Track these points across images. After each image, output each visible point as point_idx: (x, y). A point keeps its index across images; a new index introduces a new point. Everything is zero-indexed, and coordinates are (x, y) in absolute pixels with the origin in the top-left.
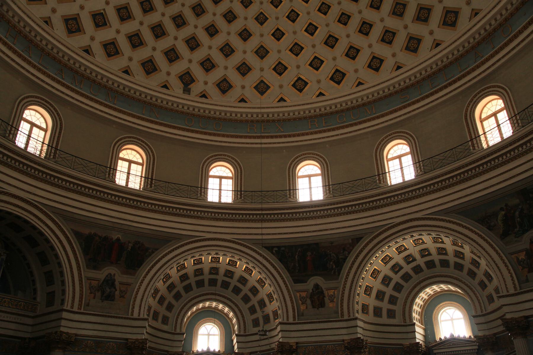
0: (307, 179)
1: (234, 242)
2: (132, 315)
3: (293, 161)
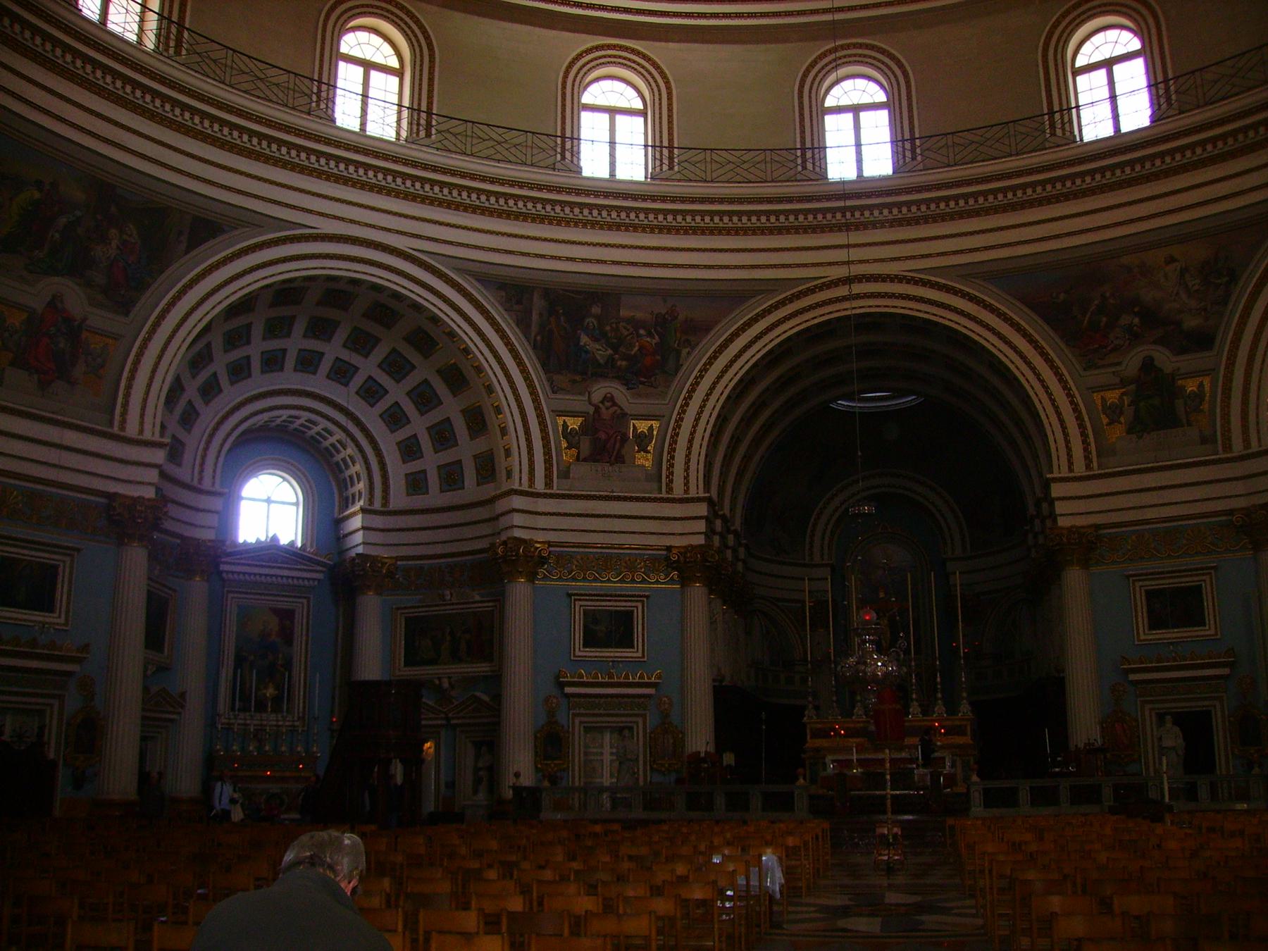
0: (1102, 73)
1: (910, 281)
2: (670, 490)
3: (1055, 26)
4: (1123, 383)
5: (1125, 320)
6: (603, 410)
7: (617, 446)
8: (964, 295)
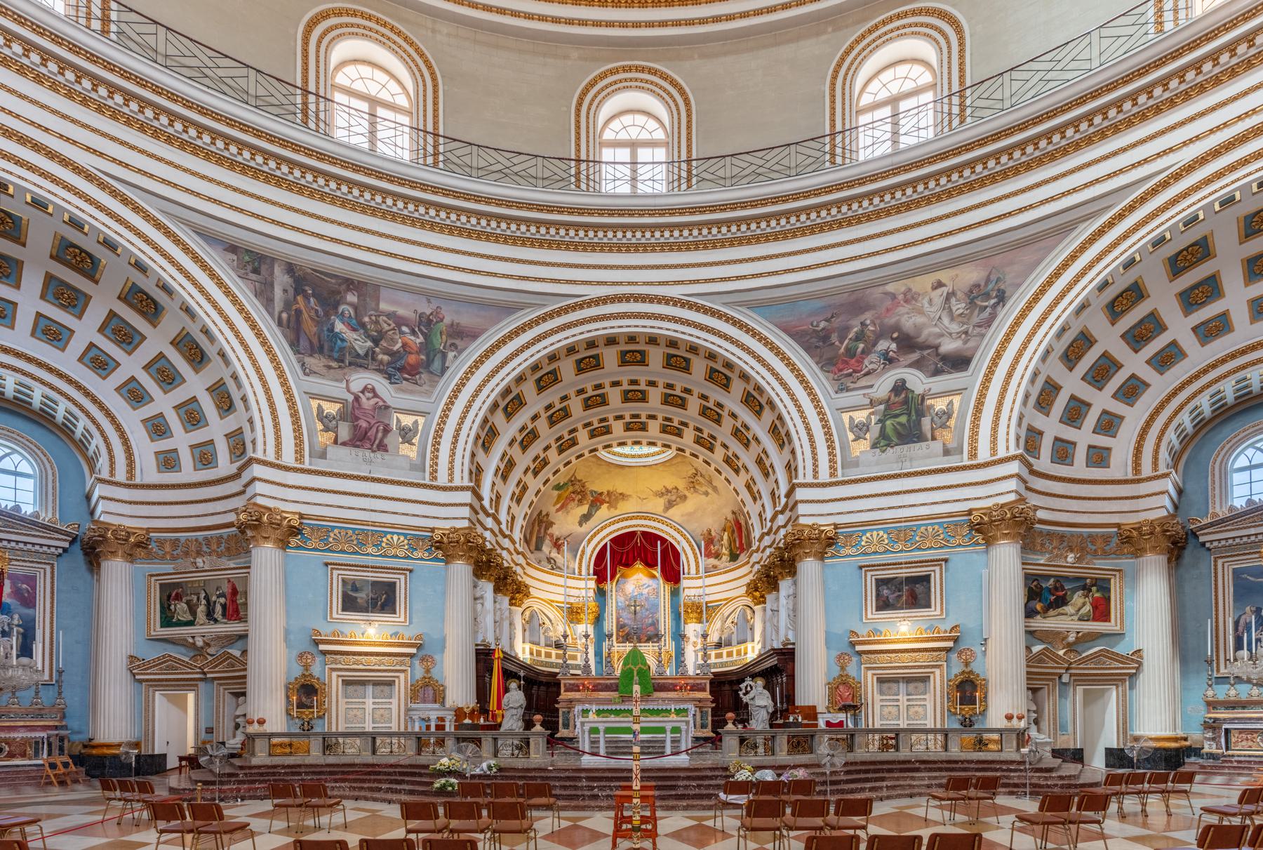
4: (872, 403)
6: (363, 399)
7: (380, 435)
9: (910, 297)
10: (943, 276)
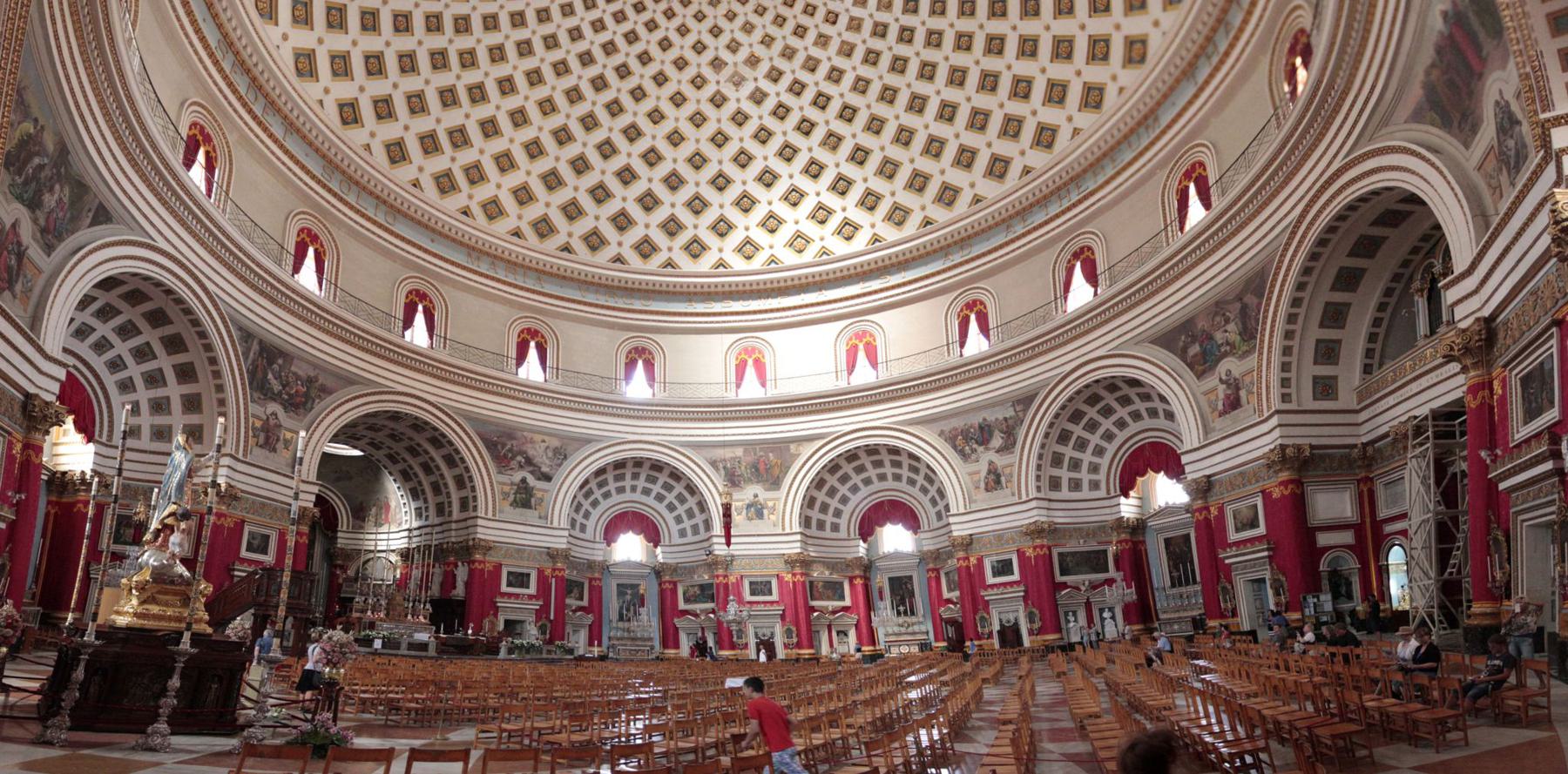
5: (519, 458)
8: (456, 422)
9: (532, 441)
10: (546, 438)
